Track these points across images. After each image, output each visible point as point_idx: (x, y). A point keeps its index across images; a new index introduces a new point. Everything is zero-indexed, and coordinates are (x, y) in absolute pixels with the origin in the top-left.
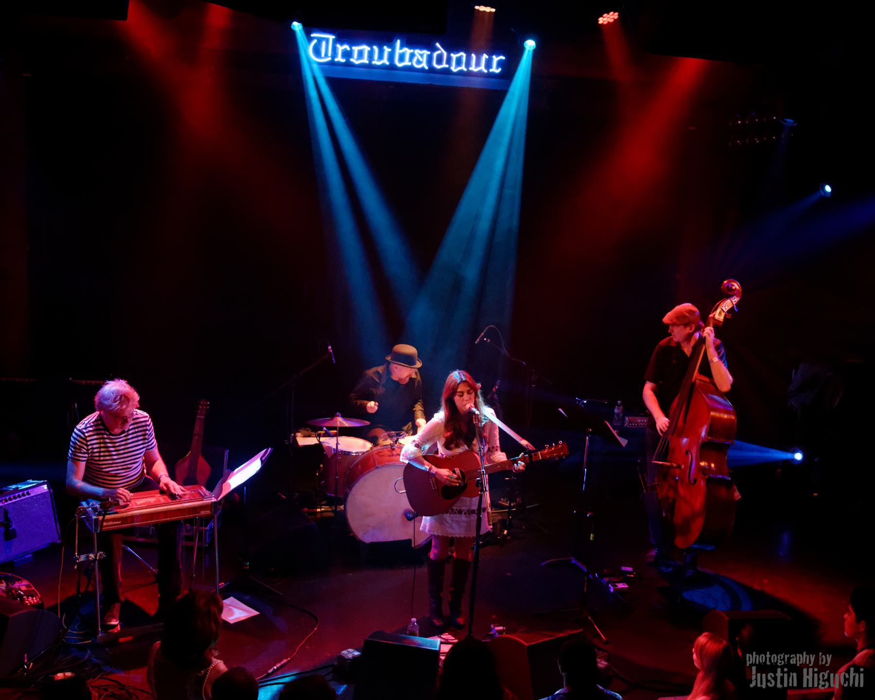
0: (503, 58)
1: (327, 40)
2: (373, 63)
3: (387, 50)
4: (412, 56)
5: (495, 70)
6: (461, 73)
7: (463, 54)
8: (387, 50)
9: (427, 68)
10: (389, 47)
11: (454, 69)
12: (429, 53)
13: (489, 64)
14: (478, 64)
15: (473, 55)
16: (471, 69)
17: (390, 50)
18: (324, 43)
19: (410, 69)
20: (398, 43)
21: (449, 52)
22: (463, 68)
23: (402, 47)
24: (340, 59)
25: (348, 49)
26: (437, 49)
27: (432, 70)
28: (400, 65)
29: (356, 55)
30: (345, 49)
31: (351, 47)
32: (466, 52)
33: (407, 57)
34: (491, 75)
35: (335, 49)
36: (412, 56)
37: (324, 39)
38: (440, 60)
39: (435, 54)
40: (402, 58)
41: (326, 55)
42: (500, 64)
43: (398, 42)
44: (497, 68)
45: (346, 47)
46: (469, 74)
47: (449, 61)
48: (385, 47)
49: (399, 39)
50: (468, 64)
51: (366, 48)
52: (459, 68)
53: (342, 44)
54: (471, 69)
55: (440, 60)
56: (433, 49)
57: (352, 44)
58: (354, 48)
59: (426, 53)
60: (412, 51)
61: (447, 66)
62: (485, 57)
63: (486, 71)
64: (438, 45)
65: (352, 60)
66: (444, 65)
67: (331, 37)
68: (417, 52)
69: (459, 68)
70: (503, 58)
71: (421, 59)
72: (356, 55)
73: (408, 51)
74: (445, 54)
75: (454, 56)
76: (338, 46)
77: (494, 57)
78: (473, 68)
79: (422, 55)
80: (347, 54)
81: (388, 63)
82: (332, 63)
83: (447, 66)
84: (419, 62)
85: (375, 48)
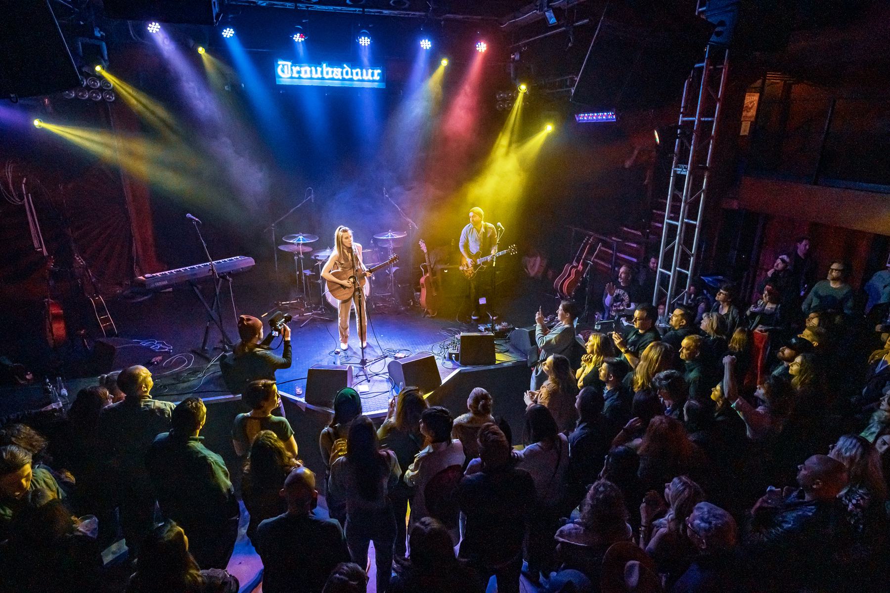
0: (379, 71)
1: (288, 66)
2: (313, 76)
3: (319, 69)
4: (333, 72)
5: (377, 78)
6: (359, 80)
7: (358, 70)
9: (341, 78)
10: (321, 67)
11: (355, 78)
12: (341, 70)
13: (373, 75)
14: (367, 75)
15: (364, 71)
18: (286, 67)
19: (333, 79)
20: (324, 65)
22: (360, 77)
23: (327, 66)
24: (295, 75)
25: (299, 70)
27: (344, 79)
32: (360, 69)
33: (330, 73)
34: (374, 81)
36: (333, 72)
37: (285, 65)
38: (347, 73)
40: (327, 73)
41: (288, 73)
42: (379, 74)
44: (378, 75)
45: (298, 68)
46: (363, 81)
47: (352, 74)
48: (318, 68)
50: (362, 75)
51: (308, 69)
55: (347, 73)
56: (343, 68)
58: (301, 69)
59: (340, 70)
63: (371, 79)
64: (345, 66)
66: (350, 76)
67: (289, 64)
68: (335, 69)
70: (379, 71)
71: (337, 74)
72: (303, 72)
73: (330, 69)
74: (349, 70)
75: (354, 71)
76: (293, 68)
78: (365, 78)
79: (337, 72)
80: (299, 72)
81: (320, 76)
82: (292, 78)
83: (351, 77)
84: (336, 75)
85: (313, 68)
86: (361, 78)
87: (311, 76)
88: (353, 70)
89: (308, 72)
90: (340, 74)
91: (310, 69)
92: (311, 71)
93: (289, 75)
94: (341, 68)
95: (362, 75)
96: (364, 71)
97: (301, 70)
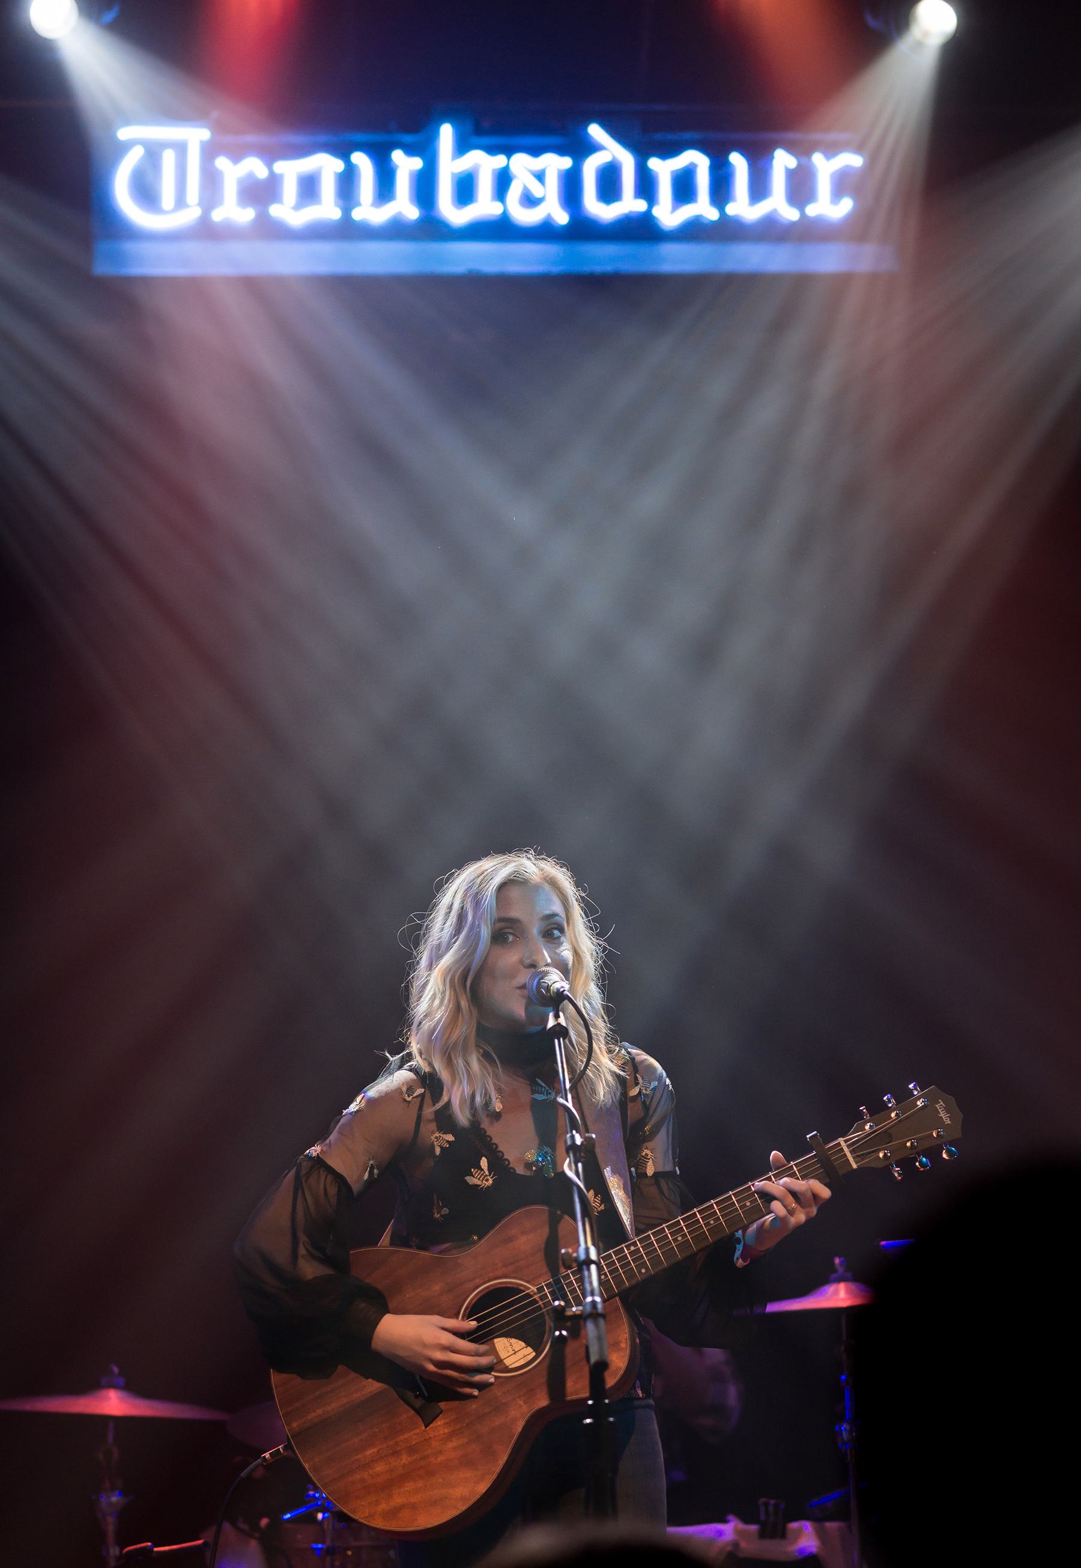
0: (853, 160)
1: (181, 148)
2: (357, 215)
3: (406, 165)
4: (503, 181)
7: (697, 160)
8: (406, 165)
9: (562, 218)
10: (411, 150)
12: (566, 162)
14: (759, 189)
15: (738, 161)
16: (731, 209)
17: (416, 163)
20: (446, 133)
21: (642, 151)
22: (703, 208)
23: (462, 147)
26: (593, 147)
28: (455, 216)
29: (290, 190)
30: (251, 176)
31: (269, 165)
32: (703, 147)
33: (485, 186)
35: (211, 180)
36: (503, 181)
37: (164, 145)
39: (591, 166)
40: (465, 190)
41: (181, 202)
42: (842, 184)
43: (446, 133)
45: (255, 167)
47: (646, 187)
48: (398, 156)
49: (445, 117)
50: (721, 190)
52: (687, 212)
53: (236, 158)
54: (731, 209)
56: (581, 149)
57: (270, 156)
58: (280, 167)
59: (555, 163)
60: (499, 161)
61: (641, 206)
62: (782, 160)
63: (791, 214)
64: (596, 131)
65: (276, 211)
66: (630, 204)
68: (521, 164)
69: (687, 212)
71: (537, 190)
72: (290, 190)
74: (627, 161)
75: (663, 169)
76: (222, 163)
77: (817, 158)
79: (540, 177)
81: (412, 213)
83: (641, 206)
84: (529, 201)
85: (361, 160)
86: (712, 214)
87: (347, 211)
88: (654, 163)
89: (328, 188)
90: (551, 193)
91: (338, 165)
92: (347, 182)
93: (191, 215)
94: (561, 151)
95: (721, 190)
96: (738, 161)
97: (272, 174)
